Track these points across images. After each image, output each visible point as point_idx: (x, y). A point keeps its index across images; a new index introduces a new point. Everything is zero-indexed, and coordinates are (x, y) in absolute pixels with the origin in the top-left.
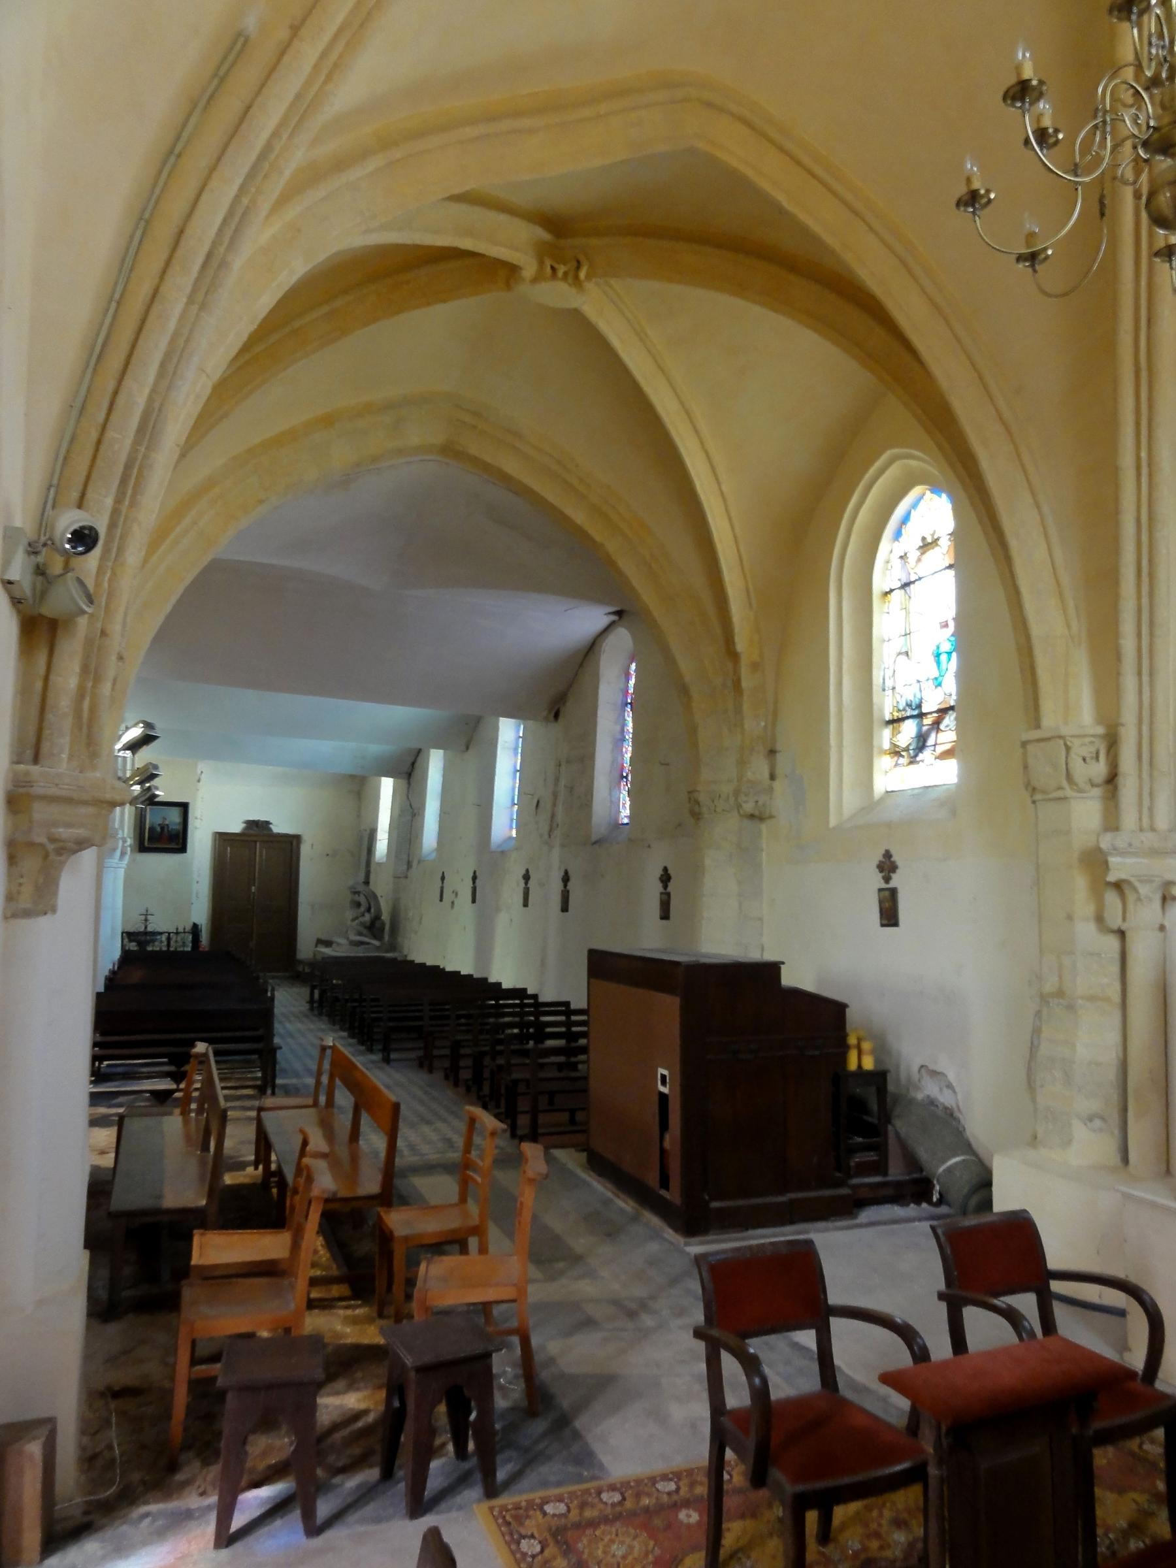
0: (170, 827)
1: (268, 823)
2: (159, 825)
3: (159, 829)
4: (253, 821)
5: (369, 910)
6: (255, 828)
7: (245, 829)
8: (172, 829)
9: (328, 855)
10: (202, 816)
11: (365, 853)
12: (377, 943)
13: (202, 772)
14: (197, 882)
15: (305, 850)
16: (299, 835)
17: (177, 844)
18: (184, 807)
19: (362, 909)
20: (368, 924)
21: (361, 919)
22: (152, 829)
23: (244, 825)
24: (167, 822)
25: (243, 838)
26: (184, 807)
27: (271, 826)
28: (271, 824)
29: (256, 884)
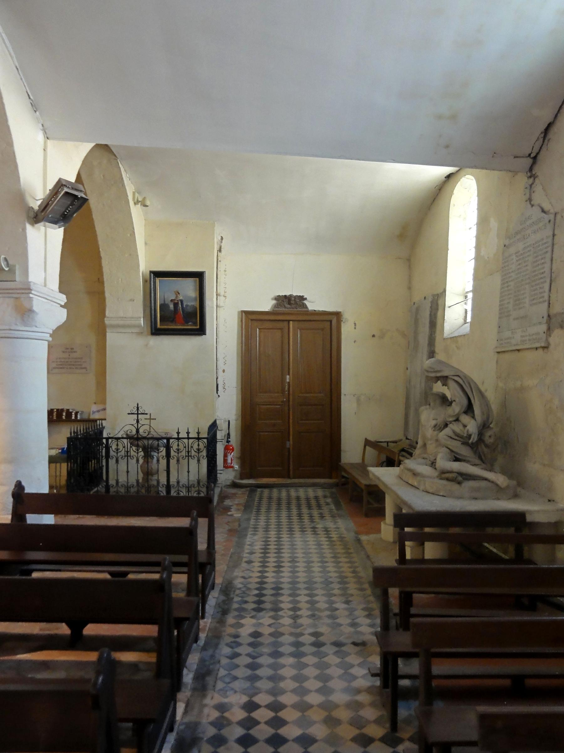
0: (185, 304)
1: (302, 298)
2: (172, 300)
3: (172, 306)
4: (285, 296)
5: (469, 409)
6: (289, 306)
7: (276, 306)
8: (187, 306)
9: (374, 336)
10: (225, 292)
11: (425, 329)
12: (501, 479)
13: (222, 238)
14: (224, 371)
15: (346, 330)
16: (340, 312)
17: (195, 324)
18: (199, 276)
19: (456, 408)
20: (474, 438)
21: (457, 428)
22: (164, 306)
23: (274, 302)
24: (181, 298)
25: (272, 317)
26: (199, 276)
27: (305, 302)
28: (306, 299)
29: (291, 372)
